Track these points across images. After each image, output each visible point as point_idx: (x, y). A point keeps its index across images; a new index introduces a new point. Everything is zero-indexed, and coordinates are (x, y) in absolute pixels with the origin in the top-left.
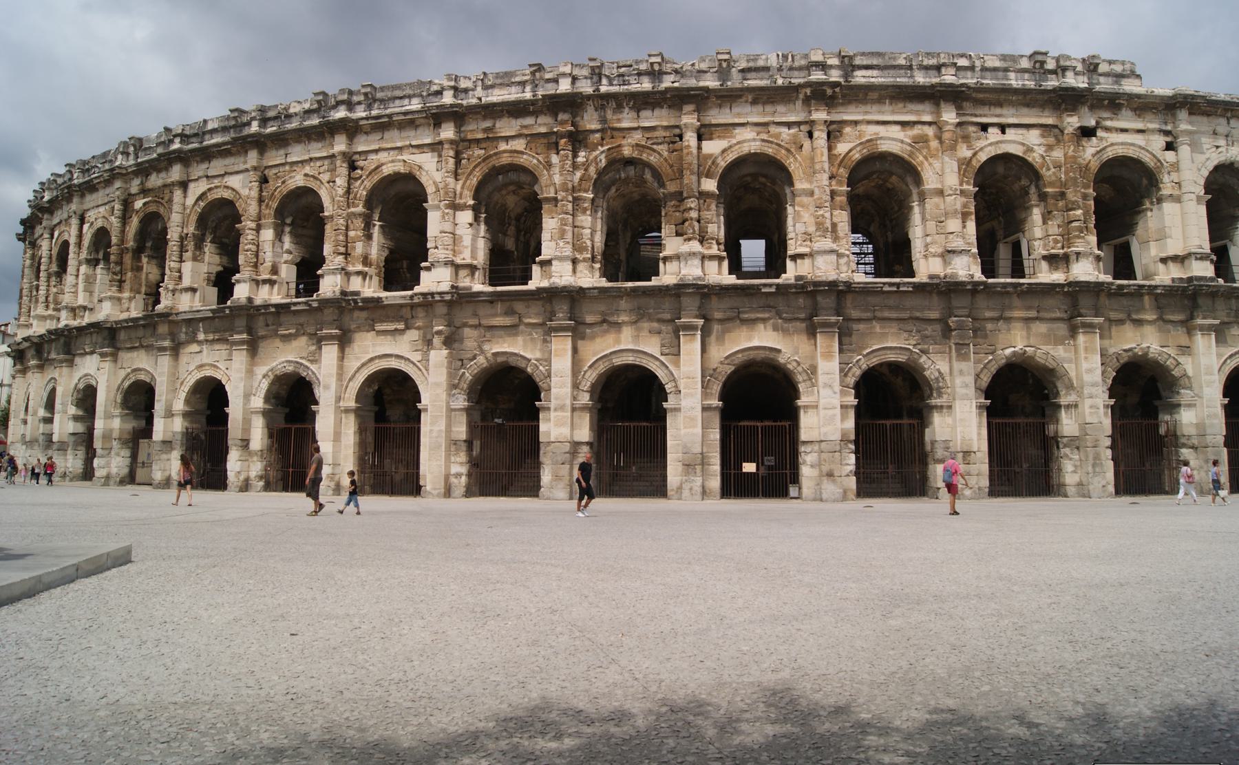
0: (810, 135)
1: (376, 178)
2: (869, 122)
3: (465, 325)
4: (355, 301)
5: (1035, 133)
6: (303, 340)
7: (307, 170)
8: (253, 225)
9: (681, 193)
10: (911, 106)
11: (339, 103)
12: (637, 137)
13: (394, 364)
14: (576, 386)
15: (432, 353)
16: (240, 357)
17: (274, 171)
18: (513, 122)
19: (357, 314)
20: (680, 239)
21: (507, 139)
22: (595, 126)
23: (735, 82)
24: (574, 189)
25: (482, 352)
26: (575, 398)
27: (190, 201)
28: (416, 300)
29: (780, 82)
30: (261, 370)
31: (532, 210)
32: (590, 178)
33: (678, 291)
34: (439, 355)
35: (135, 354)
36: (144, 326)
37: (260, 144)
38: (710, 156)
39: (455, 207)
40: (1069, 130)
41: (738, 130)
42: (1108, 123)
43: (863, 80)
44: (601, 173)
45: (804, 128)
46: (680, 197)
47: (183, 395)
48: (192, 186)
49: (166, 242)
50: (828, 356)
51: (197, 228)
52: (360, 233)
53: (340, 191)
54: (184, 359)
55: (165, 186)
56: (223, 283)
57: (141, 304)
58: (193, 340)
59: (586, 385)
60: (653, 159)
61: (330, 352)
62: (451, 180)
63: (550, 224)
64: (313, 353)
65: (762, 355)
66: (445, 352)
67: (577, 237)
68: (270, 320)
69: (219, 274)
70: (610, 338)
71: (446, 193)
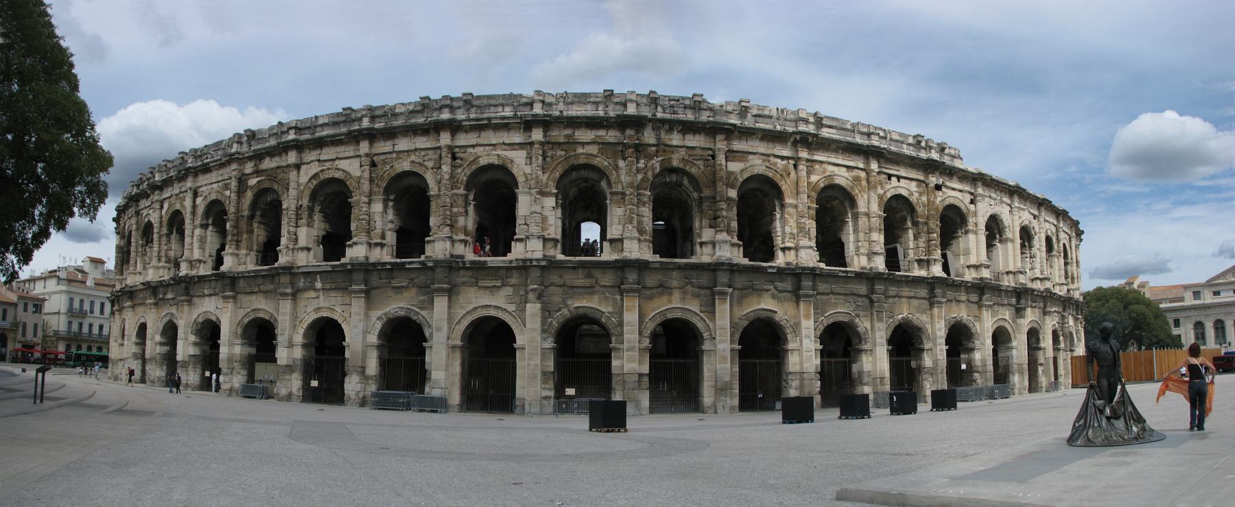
0: (795, 166)
1: (474, 167)
2: (829, 163)
3: (552, 284)
4: (464, 263)
7: (413, 158)
8: (366, 200)
9: (714, 198)
10: (854, 157)
11: (442, 107)
12: (683, 152)
13: (493, 313)
14: (640, 333)
15: (528, 305)
16: (358, 305)
17: (382, 157)
19: (462, 272)
20: (712, 231)
21: (583, 144)
23: (749, 122)
24: (638, 188)
25: (566, 306)
26: (639, 342)
29: (779, 128)
30: (376, 314)
33: (714, 268)
34: (533, 308)
35: (254, 297)
37: (371, 136)
38: (733, 173)
39: (543, 194)
41: (751, 157)
43: (827, 135)
44: (655, 177)
45: (792, 162)
46: (713, 200)
47: (301, 331)
50: (807, 317)
52: (461, 210)
53: (447, 176)
54: (301, 303)
59: (647, 333)
60: (693, 171)
61: (441, 303)
62: (540, 173)
63: (616, 213)
64: (423, 302)
65: (765, 314)
66: (539, 305)
68: (384, 275)
70: (664, 299)
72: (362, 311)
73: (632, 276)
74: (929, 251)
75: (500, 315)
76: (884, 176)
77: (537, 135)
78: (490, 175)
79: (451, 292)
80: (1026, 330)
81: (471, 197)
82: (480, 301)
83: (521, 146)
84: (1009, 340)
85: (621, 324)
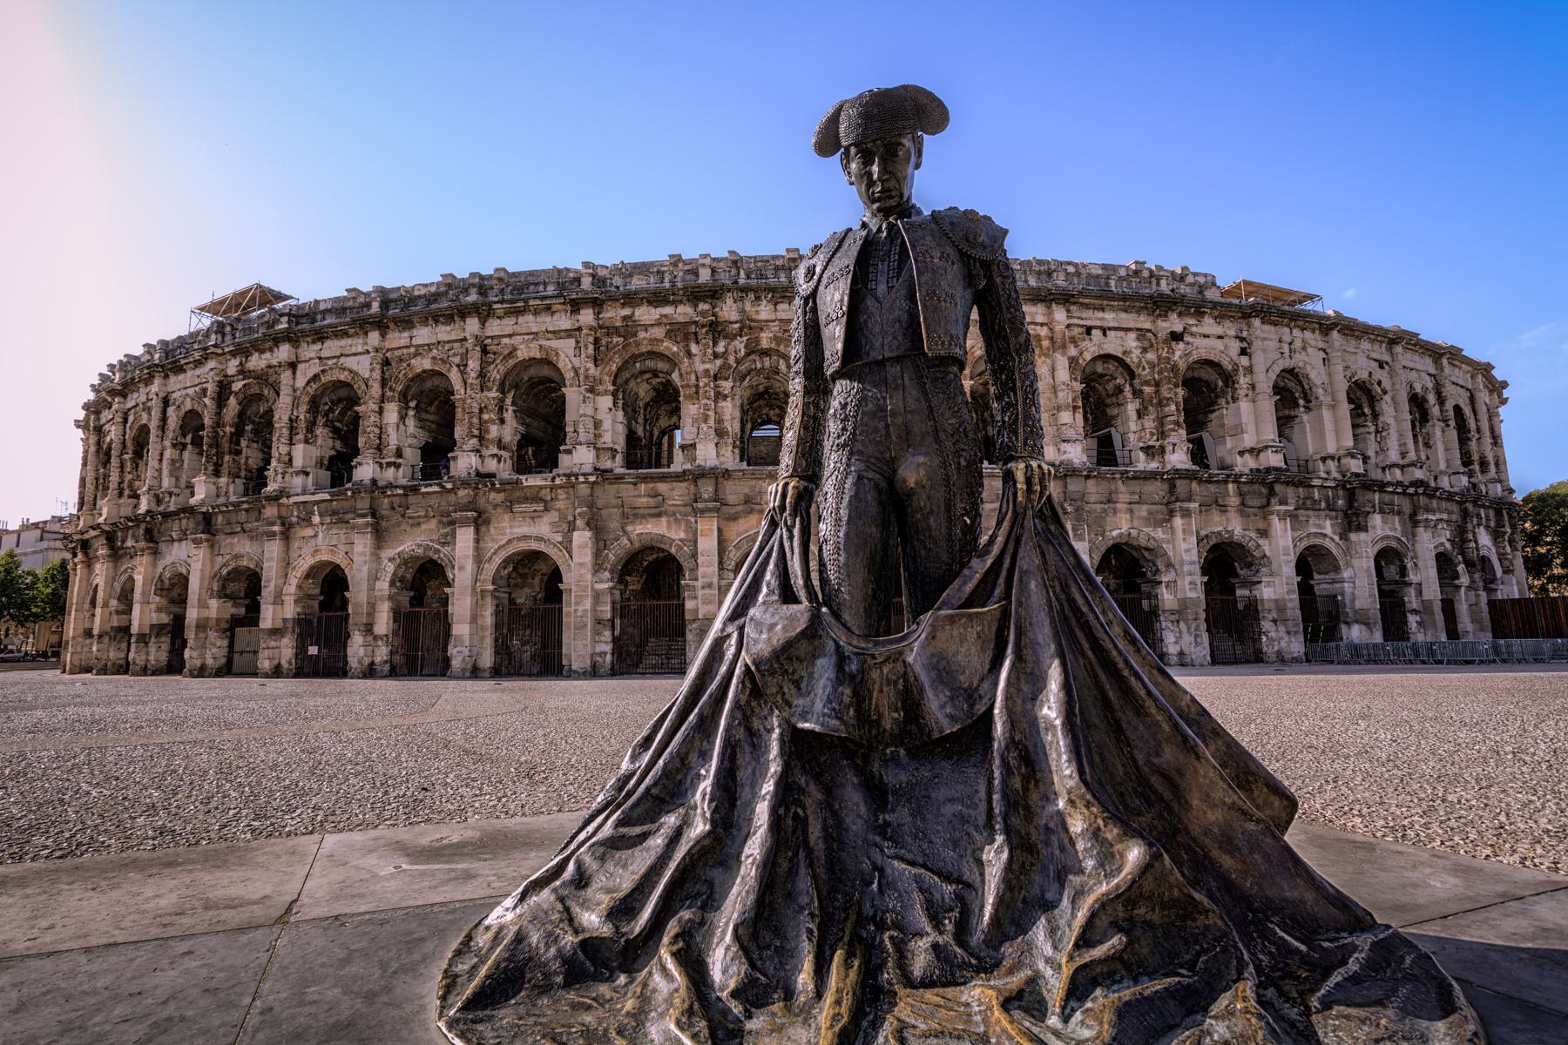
1: (511, 362)
3: (607, 506)
5: (1133, 335)
6: (433, 524)
13: (534, 546)
17: (397, 353)
18: (653, 310)
19: (493, 495)
21: (646, 327)
22: (734, 316)
24: (716, 378)
25: (625, 532)
27: (300, 383)
28: (558, 481)
31: (667, 398)
32: (730, 366)
34: (582, 537)
36: (247, 510)
37: (381, 325)
40: (1162, 335)
42: (1194, 329)
48: (301, 367)
49: (270, 424)
51: (308, 411)
53: (473, 375)
55: (269, 367)
56: (339, 467)
57: (241, 489)
58: (307, 521)
61: (465, 537)
62: (591, 365)
63: (690, 410)
64: (446, 535)
66: (588, 534)
67: (719, 421)
69: (331, 458)
71: (587, 377)
72: (368, 551)
73: (707, 489)
74: (1162, 434)
75: (542, 547)
76: (1076, 331)
77: (587, 316)
78: (533, 372)
79: (480, 522)
80: (1372, 552)
81: (509, 401)
82: (516, 531)
83: (569, 333)
84: (1337, 569)
85: (694, 555)
